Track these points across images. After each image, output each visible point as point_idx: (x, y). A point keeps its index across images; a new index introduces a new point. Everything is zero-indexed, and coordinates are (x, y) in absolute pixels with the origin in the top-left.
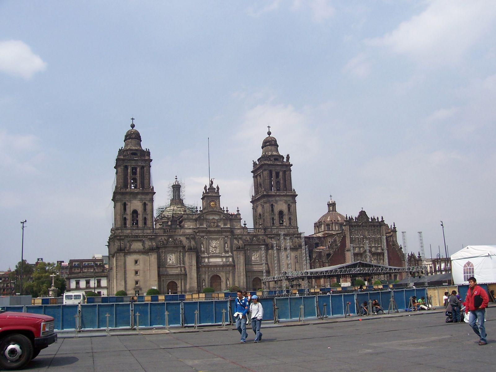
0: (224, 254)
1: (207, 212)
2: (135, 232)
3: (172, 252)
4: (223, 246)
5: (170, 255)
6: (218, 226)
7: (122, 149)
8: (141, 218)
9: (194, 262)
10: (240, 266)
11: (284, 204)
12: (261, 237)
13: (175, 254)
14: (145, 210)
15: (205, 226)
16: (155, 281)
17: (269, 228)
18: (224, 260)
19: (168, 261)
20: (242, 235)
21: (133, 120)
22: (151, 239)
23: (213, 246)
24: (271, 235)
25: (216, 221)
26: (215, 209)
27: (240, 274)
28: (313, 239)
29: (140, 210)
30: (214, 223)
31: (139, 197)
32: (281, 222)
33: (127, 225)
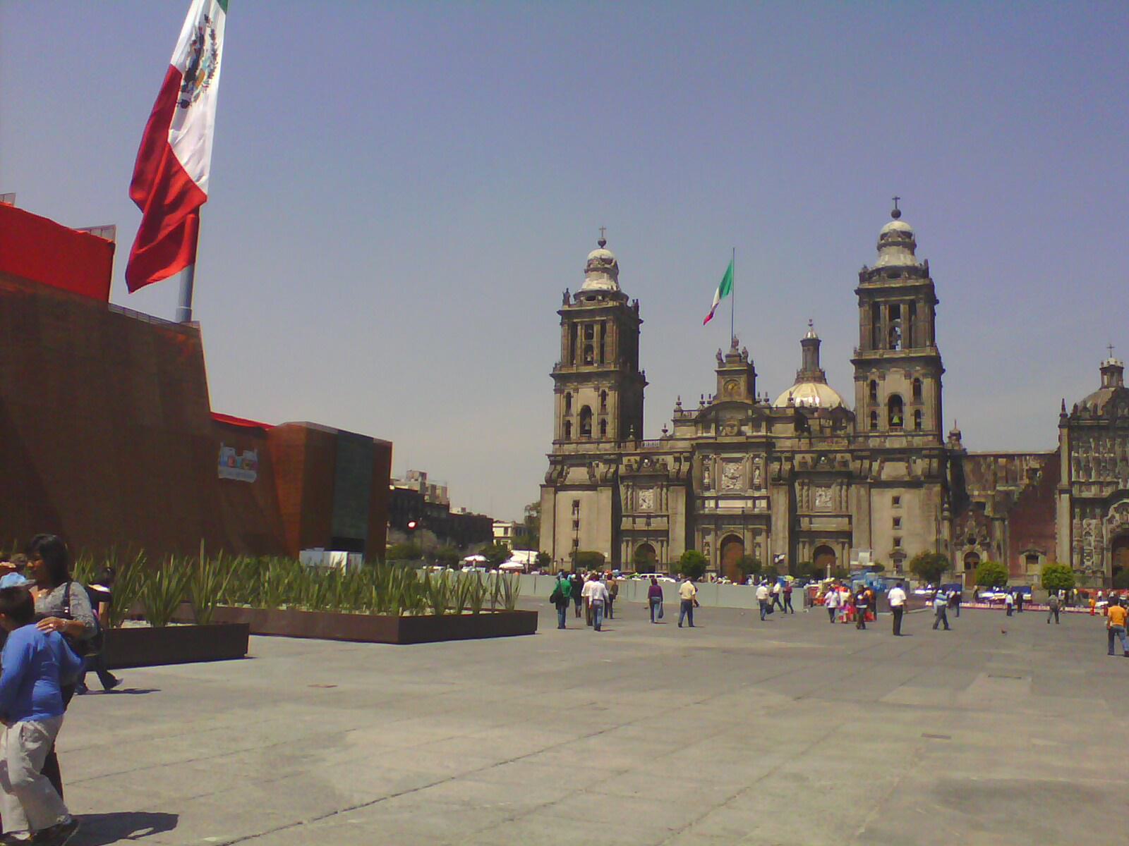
0: (750, 493)
4: (748, 475)
6: (740, 433)
7: (567, 292)
9: (682, 508)
12: (839, 456)
14: (603, 406)
15: (712, 434)
17: (861, 436)
21: (604, 231)
22: (608, 462)
23: (730, 475)
25: (736, 423)
26: (737, 397)
28: (1021, 461)
29: (595, 407)
30: (732, 426)
33: (571, 436)
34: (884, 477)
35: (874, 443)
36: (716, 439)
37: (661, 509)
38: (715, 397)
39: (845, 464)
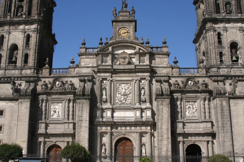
1: (113, 44)
2: (11, 74)
3: (59, 101)
5: (56, 105)
8: (21, 54)
9: (86, 116)
10: (162, 124)
11: (238, 32)
12: (201, 80)
13: (62, 103)
16: (24, 142)
18: (138, 113)
19: (51, 115)
20: (169, 77)
24: (217, 76)
25: (127, 56)
27: (162, 136)
29: (20, 43)
30: (124, 58)
31: (21, 27)
32: (234, 58)
34: (238, 93)
35: (224, 71)
36: (112, 67)
37: (68, 119)
38: (111, 39)
39: (206, 85)
